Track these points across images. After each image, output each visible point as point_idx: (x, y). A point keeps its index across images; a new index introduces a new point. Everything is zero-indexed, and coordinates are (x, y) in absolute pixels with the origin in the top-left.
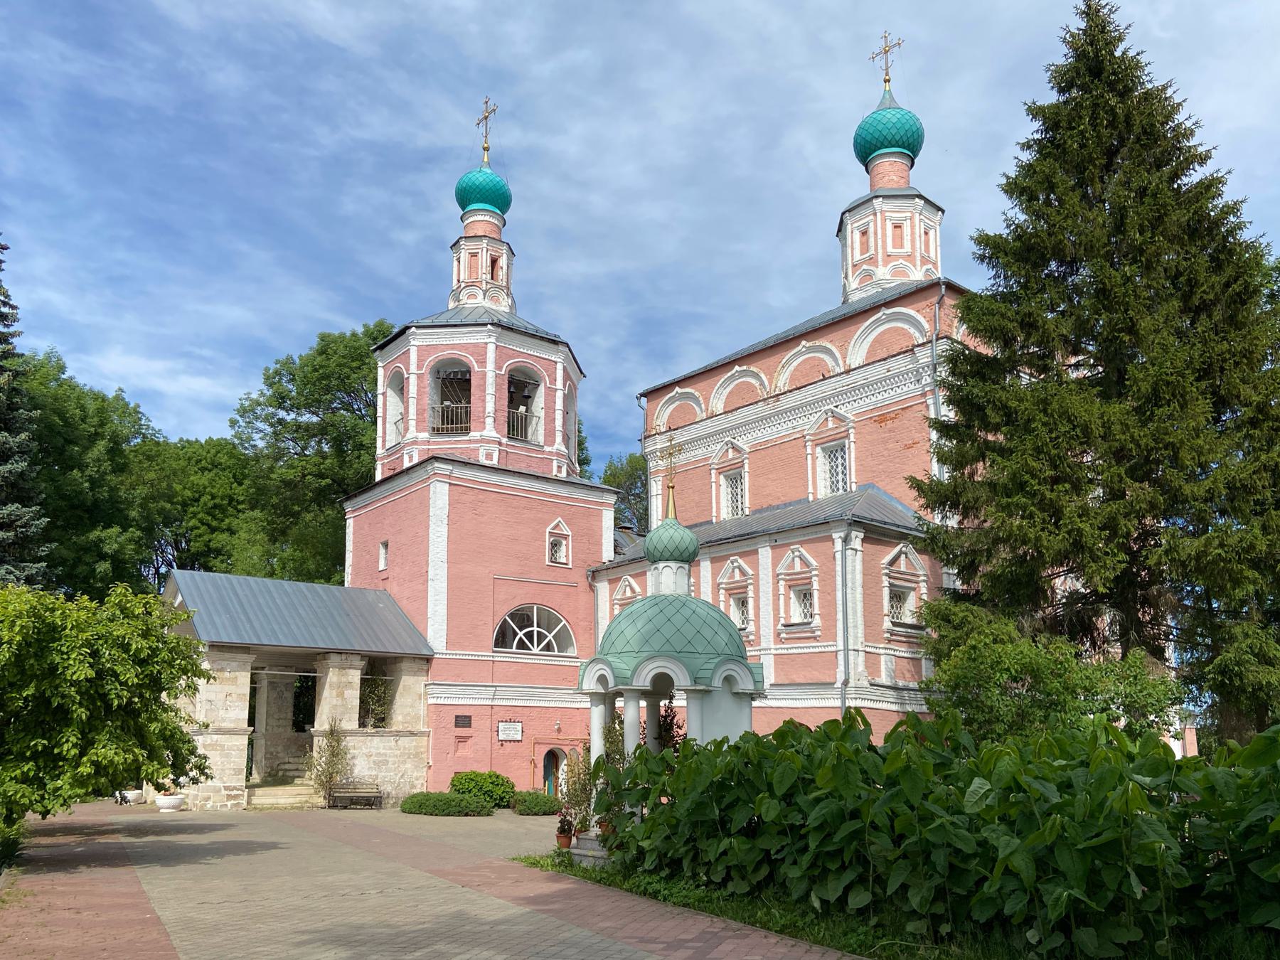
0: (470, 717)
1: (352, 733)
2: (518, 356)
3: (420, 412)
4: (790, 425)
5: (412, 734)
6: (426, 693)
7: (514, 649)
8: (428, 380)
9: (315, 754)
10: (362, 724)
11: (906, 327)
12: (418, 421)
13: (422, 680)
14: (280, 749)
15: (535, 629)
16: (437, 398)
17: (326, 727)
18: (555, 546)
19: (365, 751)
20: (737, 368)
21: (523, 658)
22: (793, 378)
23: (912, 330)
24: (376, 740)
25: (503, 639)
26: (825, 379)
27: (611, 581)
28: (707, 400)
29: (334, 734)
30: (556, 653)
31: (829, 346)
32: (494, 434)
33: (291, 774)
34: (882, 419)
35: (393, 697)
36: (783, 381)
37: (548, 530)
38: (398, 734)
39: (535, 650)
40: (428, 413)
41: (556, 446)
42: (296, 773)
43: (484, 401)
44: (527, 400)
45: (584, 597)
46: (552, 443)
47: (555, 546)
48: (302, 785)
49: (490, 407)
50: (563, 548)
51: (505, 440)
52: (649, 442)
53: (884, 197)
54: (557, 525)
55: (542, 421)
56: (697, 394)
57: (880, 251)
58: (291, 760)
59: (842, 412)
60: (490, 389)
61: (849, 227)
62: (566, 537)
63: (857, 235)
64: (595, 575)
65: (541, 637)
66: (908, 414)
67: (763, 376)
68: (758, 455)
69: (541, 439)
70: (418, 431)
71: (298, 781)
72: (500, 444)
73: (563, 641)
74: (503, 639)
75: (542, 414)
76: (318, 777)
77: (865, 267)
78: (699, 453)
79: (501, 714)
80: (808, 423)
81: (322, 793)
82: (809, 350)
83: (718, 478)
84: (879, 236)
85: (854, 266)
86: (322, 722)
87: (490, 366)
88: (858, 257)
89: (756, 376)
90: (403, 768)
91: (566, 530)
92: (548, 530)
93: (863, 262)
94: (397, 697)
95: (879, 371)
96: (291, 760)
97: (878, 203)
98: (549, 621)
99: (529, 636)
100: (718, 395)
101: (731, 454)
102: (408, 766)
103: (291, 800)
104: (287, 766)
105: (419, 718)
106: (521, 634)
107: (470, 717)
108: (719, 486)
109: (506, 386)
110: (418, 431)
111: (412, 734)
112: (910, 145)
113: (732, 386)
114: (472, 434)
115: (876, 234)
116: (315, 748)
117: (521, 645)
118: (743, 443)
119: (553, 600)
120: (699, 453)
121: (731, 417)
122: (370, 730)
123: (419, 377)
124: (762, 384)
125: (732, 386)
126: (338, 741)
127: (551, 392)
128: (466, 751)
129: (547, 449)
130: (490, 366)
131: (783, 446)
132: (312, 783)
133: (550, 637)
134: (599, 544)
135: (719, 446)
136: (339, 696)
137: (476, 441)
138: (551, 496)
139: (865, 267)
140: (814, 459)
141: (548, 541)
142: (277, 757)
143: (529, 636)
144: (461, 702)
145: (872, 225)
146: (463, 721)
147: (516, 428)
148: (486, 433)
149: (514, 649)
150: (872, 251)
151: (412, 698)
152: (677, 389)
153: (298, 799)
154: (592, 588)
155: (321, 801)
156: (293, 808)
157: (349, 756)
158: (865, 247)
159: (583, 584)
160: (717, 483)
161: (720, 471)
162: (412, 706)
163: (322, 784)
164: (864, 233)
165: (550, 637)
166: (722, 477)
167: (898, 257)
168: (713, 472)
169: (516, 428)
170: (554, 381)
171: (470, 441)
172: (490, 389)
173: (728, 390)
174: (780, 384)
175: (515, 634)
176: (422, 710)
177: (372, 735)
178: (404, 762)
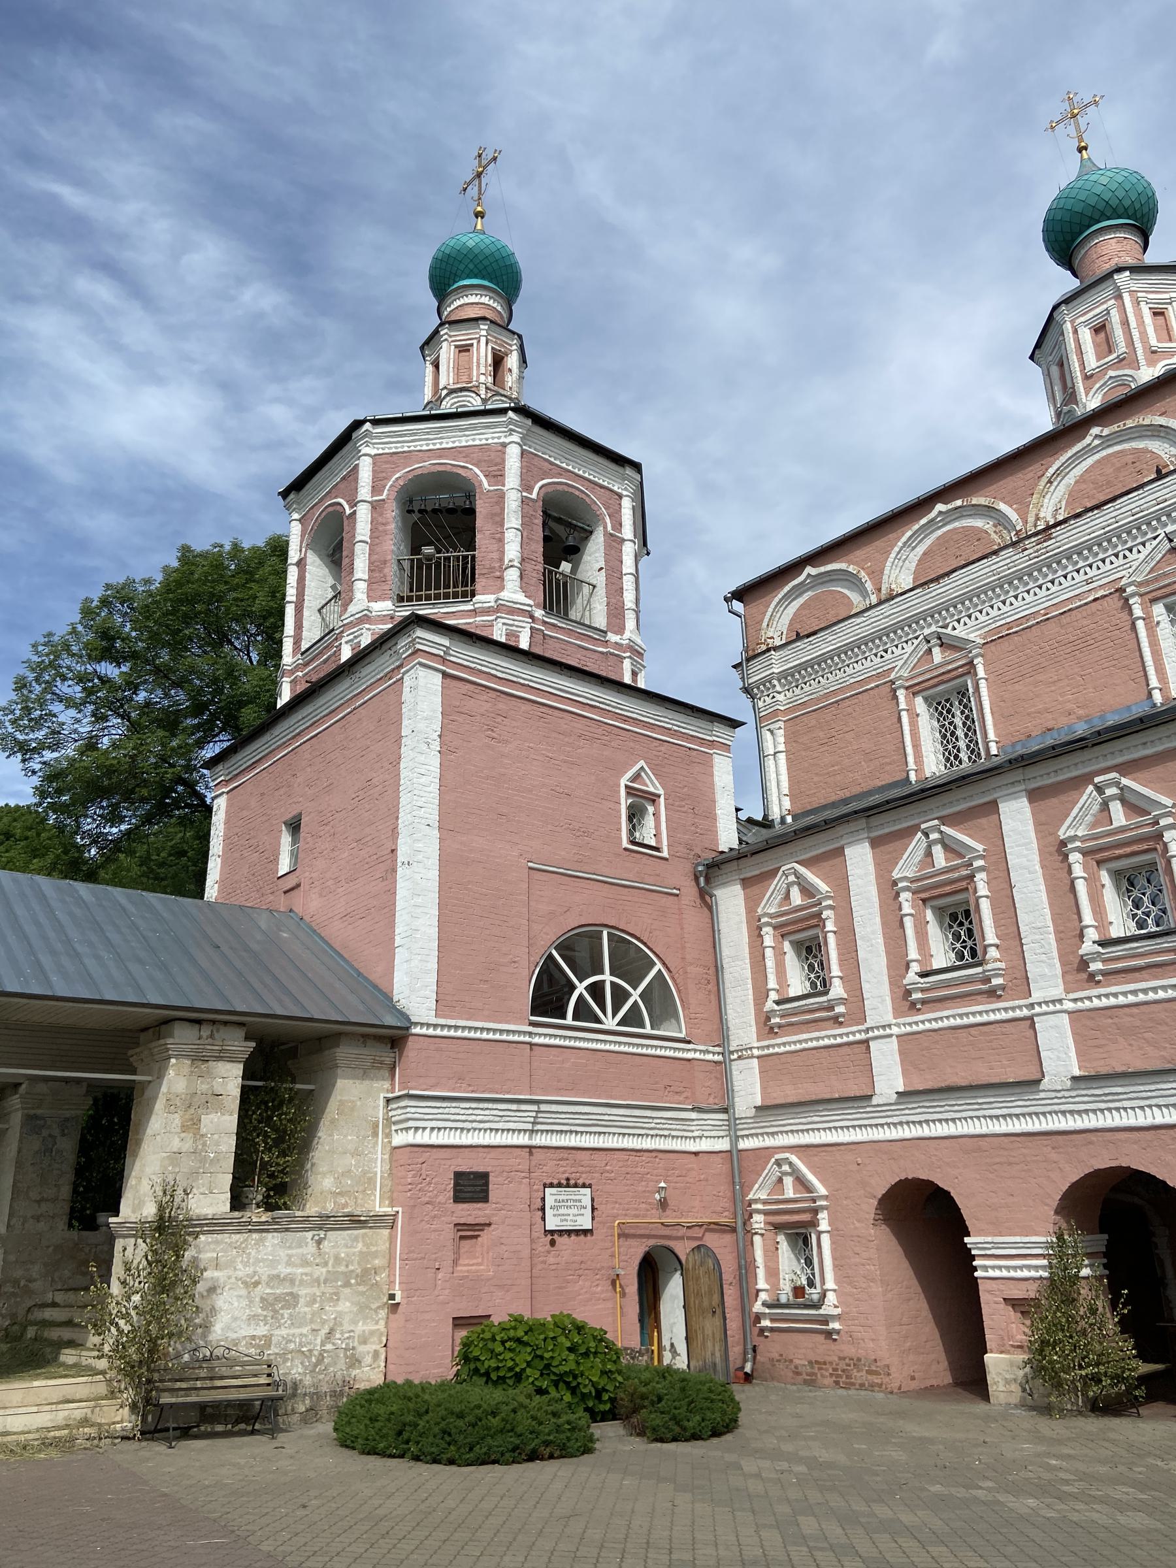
0: (485, 1176)
1: (214, 1225)
2: (560, 475)
3: (375, 567)
4: (1079, 578)
5: (355, 1222)
6: (389, 1122)
7: (569, 1020)
8: (392, 513)
9: (116, 1289)
10: (238, 1202)
12: (371, 582)
13: (381, 1089)
14: (36, 1270)
15: (607, 977)
16: (404, 548)
17: (150, 1211)
18: (635, 815)
19: (243, 1271)
20: (940, 507)
22: (1072, 496)
26: (1160, 475)
27: (746, 883)
28: (877, 575)
29: (170, 1231)
30: (648, 1030)
31: (1162, 421)
32: (521, 597)
33: (54, 1334)
35: (311, 1130)
36: (1051, 503)
38: (325, 1223)
40: (391, 570)
41: (627, 634)
42: (66, 1334)
43: (501, 540)
44: (573, 552)
45: (694, 917)
46: (621, 630)
47: (635, 815)
48: (79, 1370)
49: (512, 551)
50: (649, 821)
51: (539, 613)
52: (756, 665)
54: (636, 777)
55: (601, 591)
56: (851, 569)
57: (1138, 345)
58: (59, 1298)
60: (513, 520)
61: (1068, 327)
62: (653, 799)
63: (1086, 335)
64: (714, 869)
65: (620, 996)
67: (1002, 506)
68: (1005, 645)
69: (600, 621)
70: (371, 598)
71: (68, 1356)
72: (532, 617)
73: (660, 1002)
74: (549, 998)
75: (600, 579)
76: (119, 1349)
77: (1111, 373)
78: (865, 667)
79: (552, 1169)
81: (129, 1395)
82: (1107, 441)
83: (910, 702)
84: (1133, 323)
85: (1087, 377)
86: (138, 1202)
87: (512, 479)
88: (1092, 362)
90: (331, 1312)
91: (652, 785)
92: (624, 781)
93: (1103, 370)
94: (322, 1133)
96: (59, 1298)
98: (631, 963)
99: (596, 990)
100: (900, 565)
101: (938, 655)
102: (345, 1306)
103: (44, 1419)
104: (48, 1314)
106: (581, 988)
107: (485, 1176)
108: (914, 716)
109: (539, 521)
110: (371, 598)
111: (355, 1222)
112: (1140, 218)
113: (928, 542)
114: (478, 598)
115: (1125, 323)
116: (117, 1269)
117: (582, 1011)
118: (968, 631)
119: (641, 921)
120: (865, 667)
121: (936, 589)
122: (257, 1215)
123: (375, 506)
124: (1002, 521)
125: (928, 542)
127: (614, 542)
128: (477, 1261)
129: (613, 638)
130: (512, 479)
131: (1065, 620)
132: (103, 1364)
133: (635, 996)
134: (712, 817)
135: (909, 648)
136: (185, 1136)
137: (487, 611)
138: (626, 719)
139: (1111, 373)
140: (1152, 627)
141: (624, 802)
142: (28, 1292)
143: (596, 990)
145: (1114, 313)
146: (471, 1187)
147: (557, 596)
148: (506, 595)
149: (569, 1020)
150: (1122, 348)
151: (361, 1136)
152: (809, 570)
153: (63, 1414)
154: (705, 898)
155: (122, 1418)
156: (46, 1444)
157: (201, 1287)
159: (690, 891)
161: (913, 690)
163: (130, 1371)
164: (1100, 329)
165: (635, 996)
166: (919, 700)
168: (901, 694)
169: (557, 596)
170: (618, 525)
171: (475, 612)
172: (513, 520)
173: (920, 550)
175: (573, 987)
176: (379, 1165)
177: (262, 1229)
178: (335, 1298)
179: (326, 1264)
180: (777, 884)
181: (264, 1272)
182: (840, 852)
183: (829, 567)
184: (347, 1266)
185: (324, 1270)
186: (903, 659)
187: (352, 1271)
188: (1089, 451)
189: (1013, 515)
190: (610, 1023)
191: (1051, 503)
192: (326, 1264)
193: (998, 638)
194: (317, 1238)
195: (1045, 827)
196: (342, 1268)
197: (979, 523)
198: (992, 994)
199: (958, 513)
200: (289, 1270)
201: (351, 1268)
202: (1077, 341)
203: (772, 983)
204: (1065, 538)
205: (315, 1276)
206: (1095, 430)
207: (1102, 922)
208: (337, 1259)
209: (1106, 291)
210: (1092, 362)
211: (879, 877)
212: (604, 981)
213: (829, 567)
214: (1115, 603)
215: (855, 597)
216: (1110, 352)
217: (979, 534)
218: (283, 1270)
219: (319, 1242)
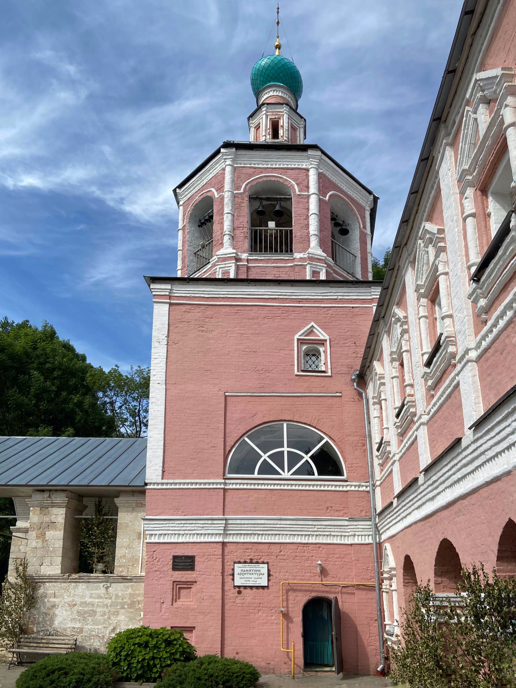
21: (268, 484)
24: (82, 586)
25: (244, 464)
37: (297, 337)
39: (286, 475)
54: (311, 332)
92: (297, 337)
105: (137, 560)
117: (266, 469)
126: (34, 589)
143: (278, 458)
144: (181, 540)
146: (184, 563)
162: (128, 547)
179: (111, 598)
181: (78, 600)
184: (123, 600)
185: (110, 601)
187: (125, 602)
190: (286, 475)
192: (111, 598)
194: (106, 586)
196: (120, 600)
200: (91, 600)
201: (125, 600)
205: (105, 603)
208: (117, 596)
212: (283, 452)
218: (88, 600)
219: (107, 588)
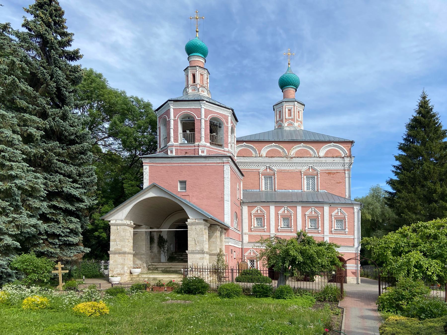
11: (339, 150)
20: (273, 144)
22: (296, 153)
23: (341, 152)
34: (329, 173)
36: (293, 152)
53: (298, 102)
59: (316, 168)
66: (338, 174)
80: (304, 169)
85: (285, 119)
88: (287, 117)
89: (282, 149)
95: (330, 160)
97: (296, 103)
108: (262, 179)
113: (270, 149)
124: (284, 151)
140: (304, 179)
158: (290, 115)
160: (262, 178)
161: (262, 175)
164: (289, 110)
167: (289, 119)
173: (268, 150)
174: (292, 154)
180: (256, 209)
182: (269, 206)
183: (250, 145)
186: (262, 169)
188: (300, 147)
189: (287, 152)
191: (293, 152)
193: (280, 172)
195: (303, 211)
197: (280, 150)
198: (291, 232)
199: (276, 146)
202: (285, 110)
203: (253, 224)
204: (295, 160)
206: (302, 144)
207: (308, 226)
209: (292, 104)
210: (287, 117)
211: (275, 212)
213: (250, 145)
214: (299, 173)
215: (253, 153)
216: (290, 116)
217: (279, 152)
